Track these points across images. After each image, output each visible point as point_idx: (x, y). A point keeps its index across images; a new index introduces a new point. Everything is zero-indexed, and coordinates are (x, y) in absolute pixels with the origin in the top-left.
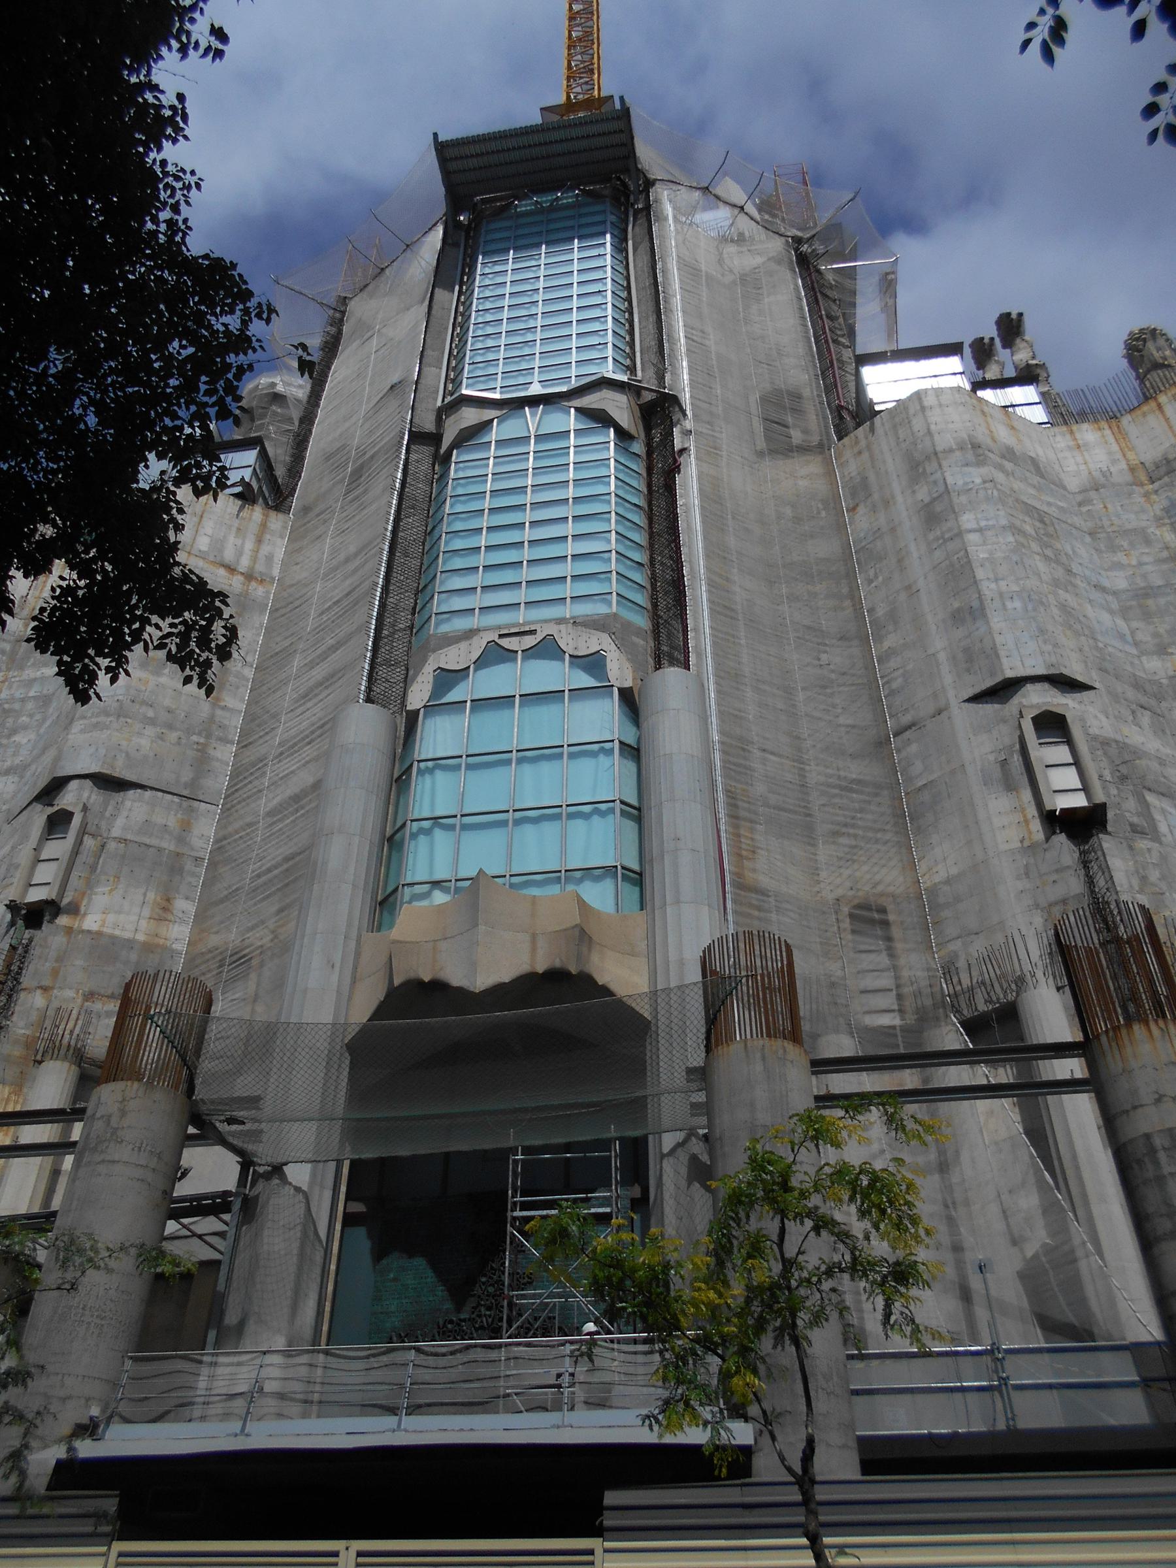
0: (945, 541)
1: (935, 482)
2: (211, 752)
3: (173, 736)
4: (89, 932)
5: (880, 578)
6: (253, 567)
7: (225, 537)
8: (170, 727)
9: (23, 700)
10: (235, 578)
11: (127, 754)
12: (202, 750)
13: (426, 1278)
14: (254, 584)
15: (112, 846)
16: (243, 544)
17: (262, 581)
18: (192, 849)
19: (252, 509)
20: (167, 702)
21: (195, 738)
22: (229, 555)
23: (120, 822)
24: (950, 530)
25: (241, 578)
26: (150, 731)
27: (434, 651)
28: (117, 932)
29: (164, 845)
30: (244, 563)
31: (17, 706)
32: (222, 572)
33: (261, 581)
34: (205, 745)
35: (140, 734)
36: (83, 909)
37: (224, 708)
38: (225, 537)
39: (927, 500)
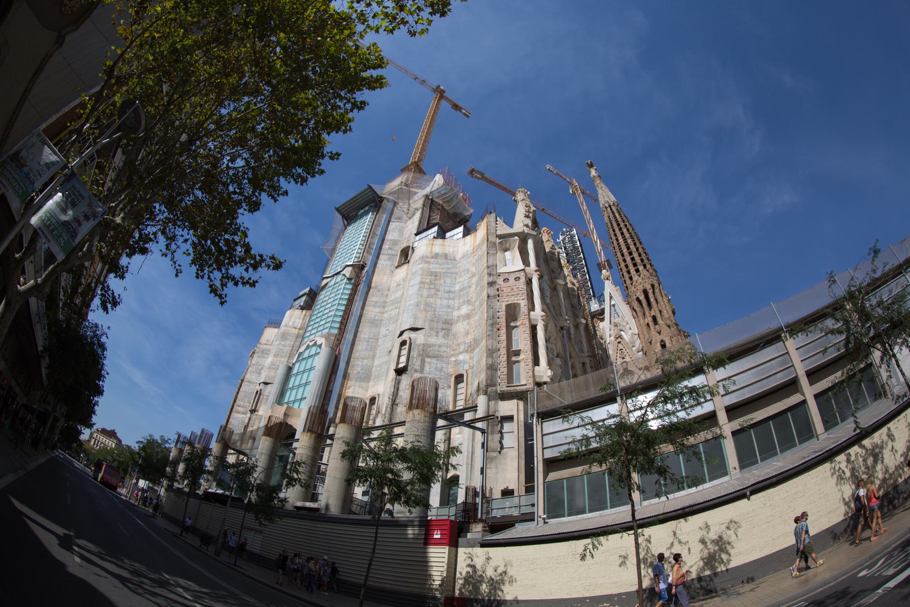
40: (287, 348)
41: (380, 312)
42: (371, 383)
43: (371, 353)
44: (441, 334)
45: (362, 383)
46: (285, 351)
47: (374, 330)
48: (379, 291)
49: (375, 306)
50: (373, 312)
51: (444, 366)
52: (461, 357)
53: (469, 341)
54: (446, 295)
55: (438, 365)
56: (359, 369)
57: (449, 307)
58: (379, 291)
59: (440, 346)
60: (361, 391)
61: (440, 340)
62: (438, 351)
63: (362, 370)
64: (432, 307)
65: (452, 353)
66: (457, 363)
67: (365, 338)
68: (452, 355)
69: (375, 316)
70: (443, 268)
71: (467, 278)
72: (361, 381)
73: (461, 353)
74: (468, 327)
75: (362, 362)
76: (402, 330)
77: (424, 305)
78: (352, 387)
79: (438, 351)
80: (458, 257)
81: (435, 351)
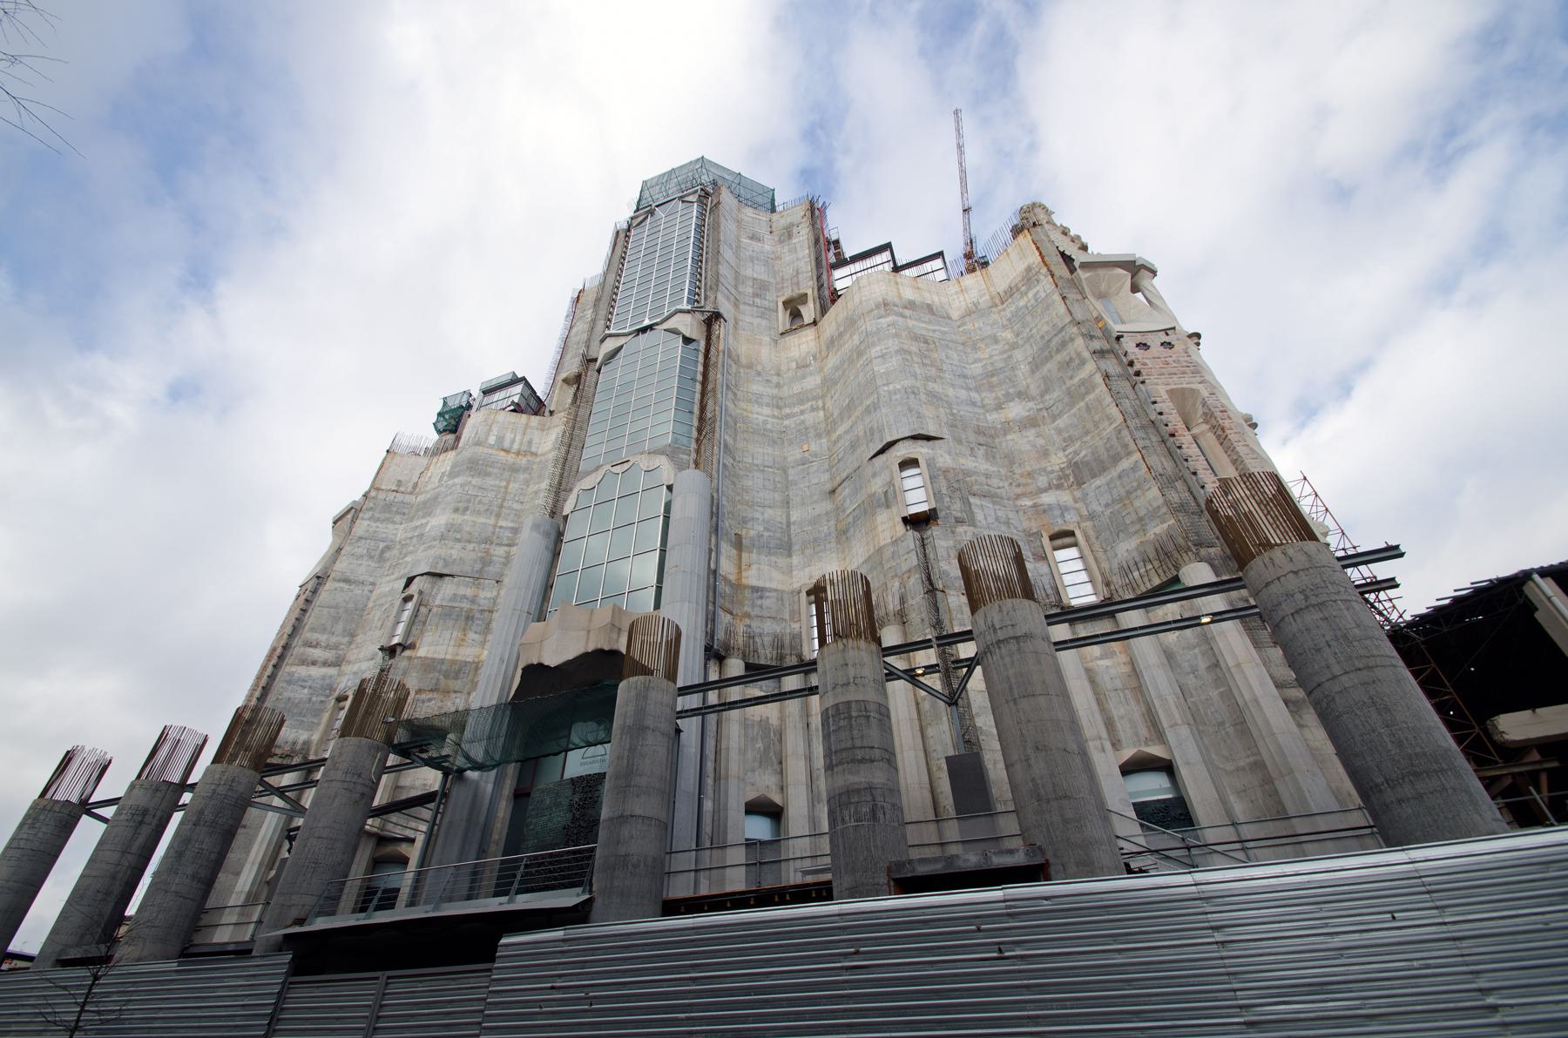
2: (491, 551)
3: (471, 546)
4: (420, 657)
8: (469, 542)
9: (411, 538)
11: (444, 560)
12: (487, 552)
15: (435, 610)
18: (479, 606)
20: (468, 529)
21: (483, 546)
22: (506, 445)
23: (439, 597)
25: (513, 455)
26: (458, 546)
28: (435, 656)
29: (464, 605)
31: (408, 541)
32: (502, 453)
34: (489, 549)
35: (452, 548)
36: (418, 646)
37: (501, 527)
40: (491, 495)
41: (774, 416)
42: (796, 559)
43: (777, 496)
44: (981, 452)
45: (773, 558)
46: (486, 500)
47: (770, 450)
48: (759, 374)
49: (760, 404)
50: (757, 413)
51: (1011, 515)
52: (1047, 499)
53: (1057, 468)
54: (960, 381)
55: (1000, 514)
56: (761, 528)
57: (974, 404)
58: (759, 374)
59: (987, 476)
60: (776, 575)
61: (983, 466)
62: (988, 485)
63: (766, 529)
64: (941, 399)
65: (1019, 490)
66: (1040, 511)
67: (757, 466)
68: (1019, 495)
69: (765, 422)
70: (934, 331)
71: (997, 352)
72: (770, 554)
73: (1045, 490)
74: (1041, 442)
75: (763, 514)
76: (890, 439)
77: (927, 394)
78: (754, 567)
79: (988, 485)
80: (955, 315)
81: (981, 484)
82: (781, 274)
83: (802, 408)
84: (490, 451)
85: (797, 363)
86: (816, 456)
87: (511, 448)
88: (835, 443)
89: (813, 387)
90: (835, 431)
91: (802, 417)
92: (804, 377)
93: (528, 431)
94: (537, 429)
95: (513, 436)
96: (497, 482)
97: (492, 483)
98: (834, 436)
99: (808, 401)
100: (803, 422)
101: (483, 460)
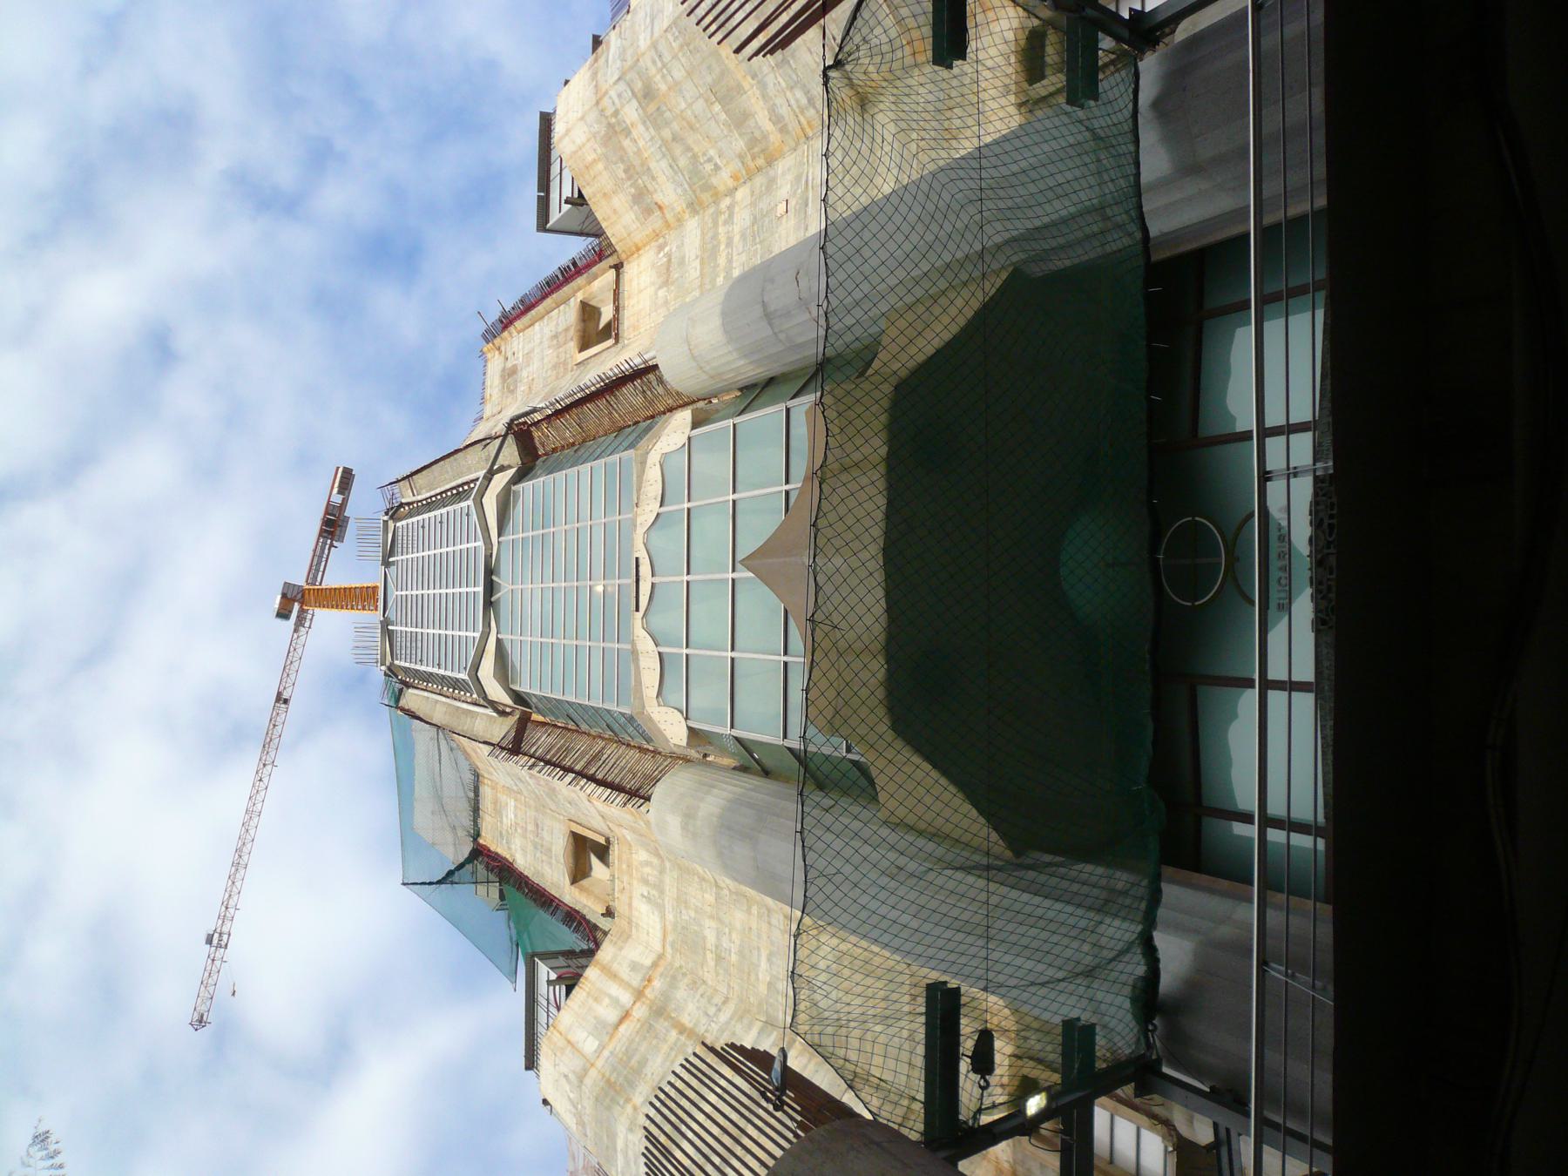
0: (664, 66)
1: (619, 96)
5: (712, 152)
6: (634, 989)
7: (595, 1018)
10: (634, 1014)
13: (646, 330)
14: (648, 992)
16: (610, 997)
17: (649, 981)
19: (586, 979)
22: (612, 1016)
24: (654, 62)
27: (644, 707)
30: (626, 998)
32: (622, 1028)
33: (649, 981)
38: (595, 1018)
39: (635, 103)
82: (549, 373)
83: (722, 247)
84: (606, 1053)
85: (660, 288)
86: (798, 178)
87: (622, 1006)
88: (783, 130)
89: (699, 233)
90: (765, 137)
91: (737, 239)
92: (682, 262)
93: (615, 967)
94: (621, 949)
95: (607, 1001)
96: (665, 1048)
97: (659, 1060)
98: (775, 138)
99: (715, 237)
100: (743, 236)
101: (614, 1069)
